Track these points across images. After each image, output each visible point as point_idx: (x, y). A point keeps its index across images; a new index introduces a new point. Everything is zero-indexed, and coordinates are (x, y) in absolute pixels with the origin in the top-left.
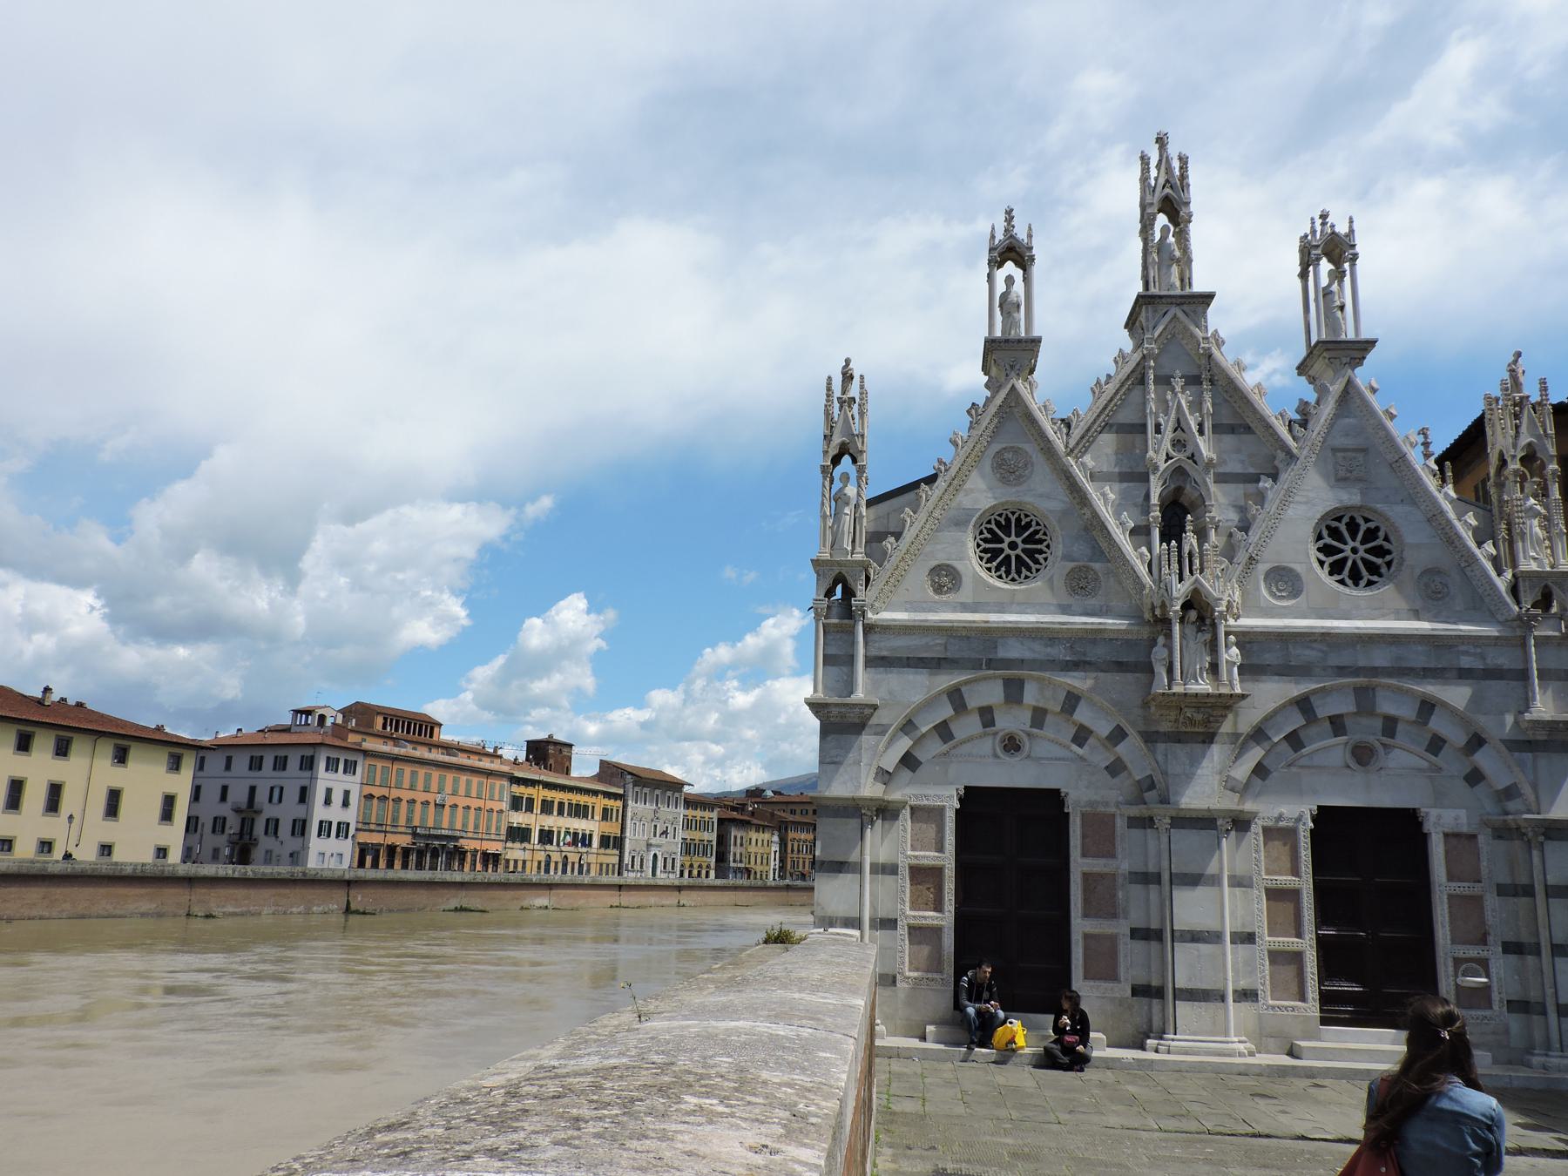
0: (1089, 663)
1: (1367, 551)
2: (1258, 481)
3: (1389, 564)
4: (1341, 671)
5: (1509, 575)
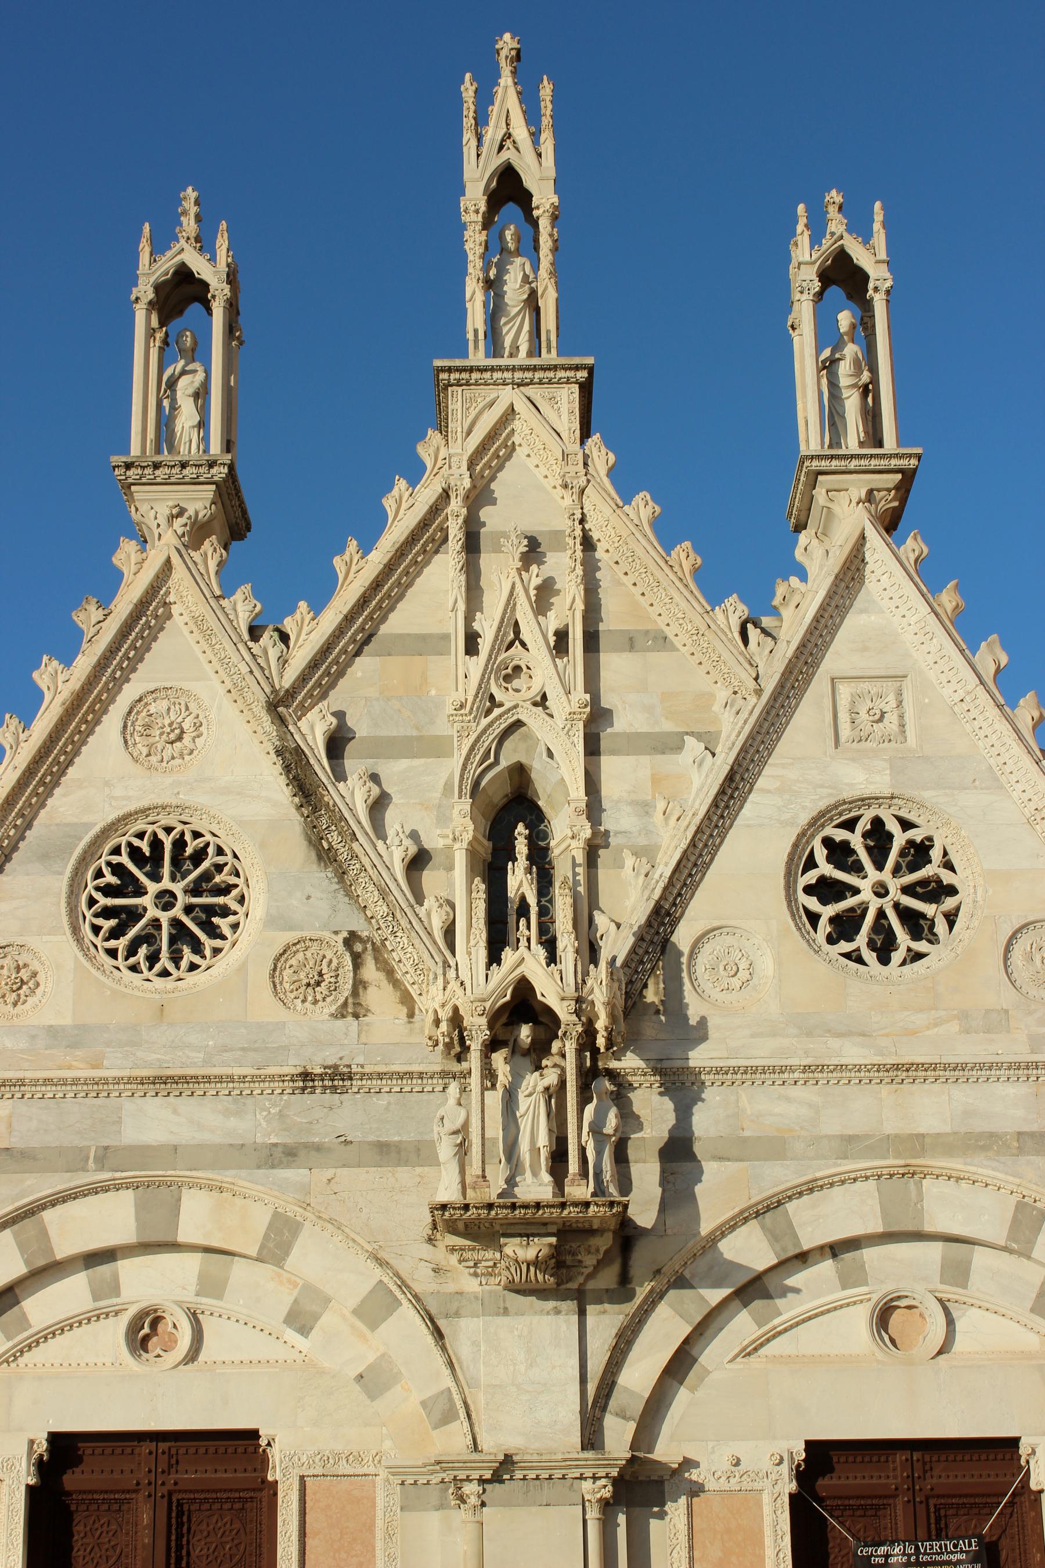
0: (318, 1148)
1: (907, 890)
2: (679, 747)
3: (951, 919)
4: (849, 1144)
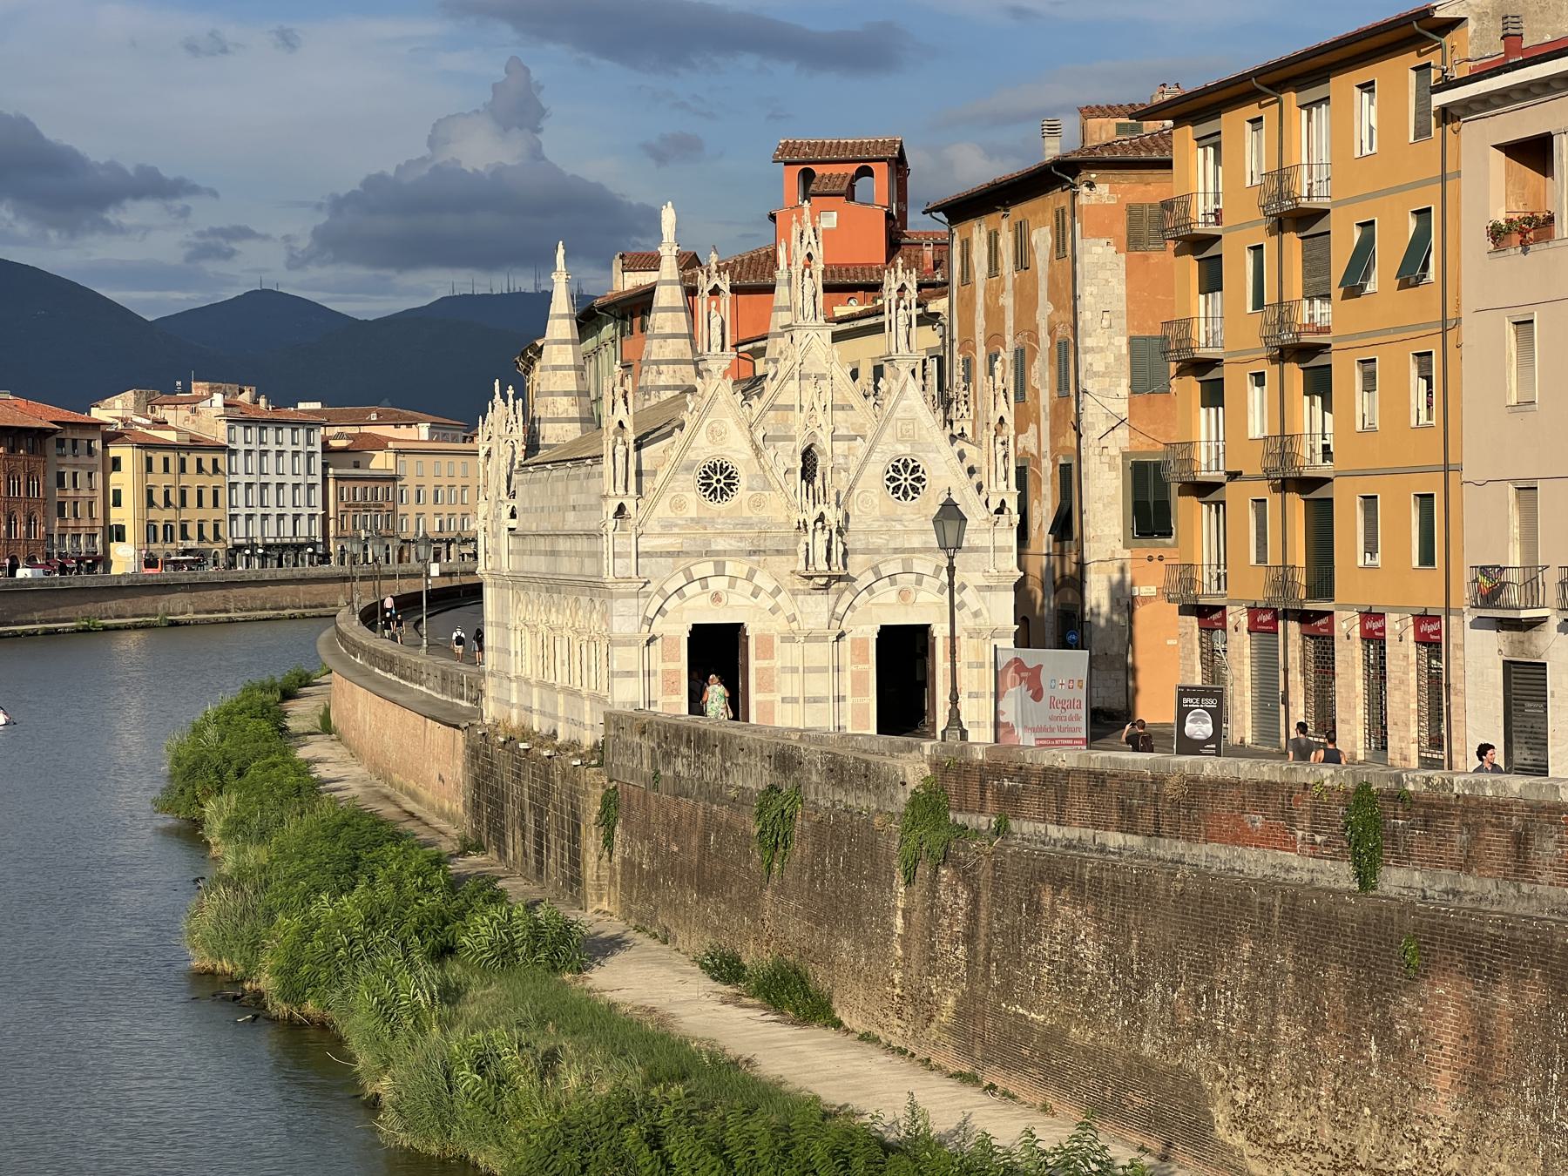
4: (896, 551)
5: (983, 497)
